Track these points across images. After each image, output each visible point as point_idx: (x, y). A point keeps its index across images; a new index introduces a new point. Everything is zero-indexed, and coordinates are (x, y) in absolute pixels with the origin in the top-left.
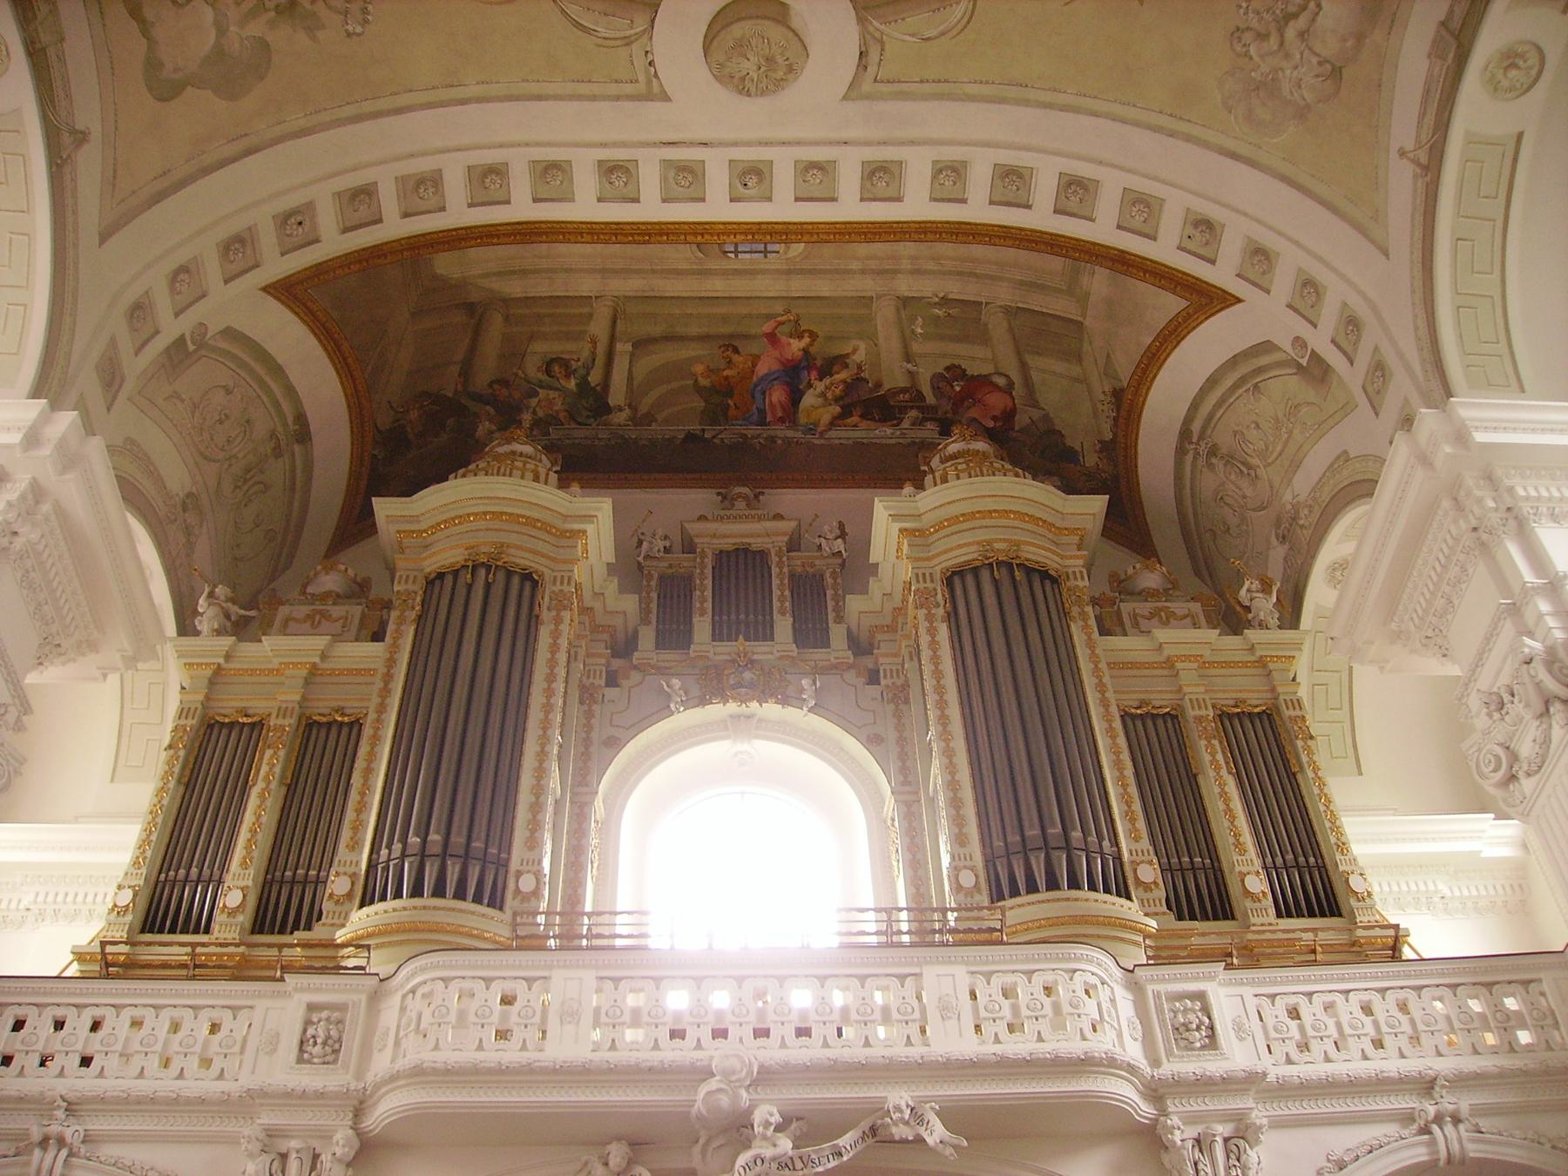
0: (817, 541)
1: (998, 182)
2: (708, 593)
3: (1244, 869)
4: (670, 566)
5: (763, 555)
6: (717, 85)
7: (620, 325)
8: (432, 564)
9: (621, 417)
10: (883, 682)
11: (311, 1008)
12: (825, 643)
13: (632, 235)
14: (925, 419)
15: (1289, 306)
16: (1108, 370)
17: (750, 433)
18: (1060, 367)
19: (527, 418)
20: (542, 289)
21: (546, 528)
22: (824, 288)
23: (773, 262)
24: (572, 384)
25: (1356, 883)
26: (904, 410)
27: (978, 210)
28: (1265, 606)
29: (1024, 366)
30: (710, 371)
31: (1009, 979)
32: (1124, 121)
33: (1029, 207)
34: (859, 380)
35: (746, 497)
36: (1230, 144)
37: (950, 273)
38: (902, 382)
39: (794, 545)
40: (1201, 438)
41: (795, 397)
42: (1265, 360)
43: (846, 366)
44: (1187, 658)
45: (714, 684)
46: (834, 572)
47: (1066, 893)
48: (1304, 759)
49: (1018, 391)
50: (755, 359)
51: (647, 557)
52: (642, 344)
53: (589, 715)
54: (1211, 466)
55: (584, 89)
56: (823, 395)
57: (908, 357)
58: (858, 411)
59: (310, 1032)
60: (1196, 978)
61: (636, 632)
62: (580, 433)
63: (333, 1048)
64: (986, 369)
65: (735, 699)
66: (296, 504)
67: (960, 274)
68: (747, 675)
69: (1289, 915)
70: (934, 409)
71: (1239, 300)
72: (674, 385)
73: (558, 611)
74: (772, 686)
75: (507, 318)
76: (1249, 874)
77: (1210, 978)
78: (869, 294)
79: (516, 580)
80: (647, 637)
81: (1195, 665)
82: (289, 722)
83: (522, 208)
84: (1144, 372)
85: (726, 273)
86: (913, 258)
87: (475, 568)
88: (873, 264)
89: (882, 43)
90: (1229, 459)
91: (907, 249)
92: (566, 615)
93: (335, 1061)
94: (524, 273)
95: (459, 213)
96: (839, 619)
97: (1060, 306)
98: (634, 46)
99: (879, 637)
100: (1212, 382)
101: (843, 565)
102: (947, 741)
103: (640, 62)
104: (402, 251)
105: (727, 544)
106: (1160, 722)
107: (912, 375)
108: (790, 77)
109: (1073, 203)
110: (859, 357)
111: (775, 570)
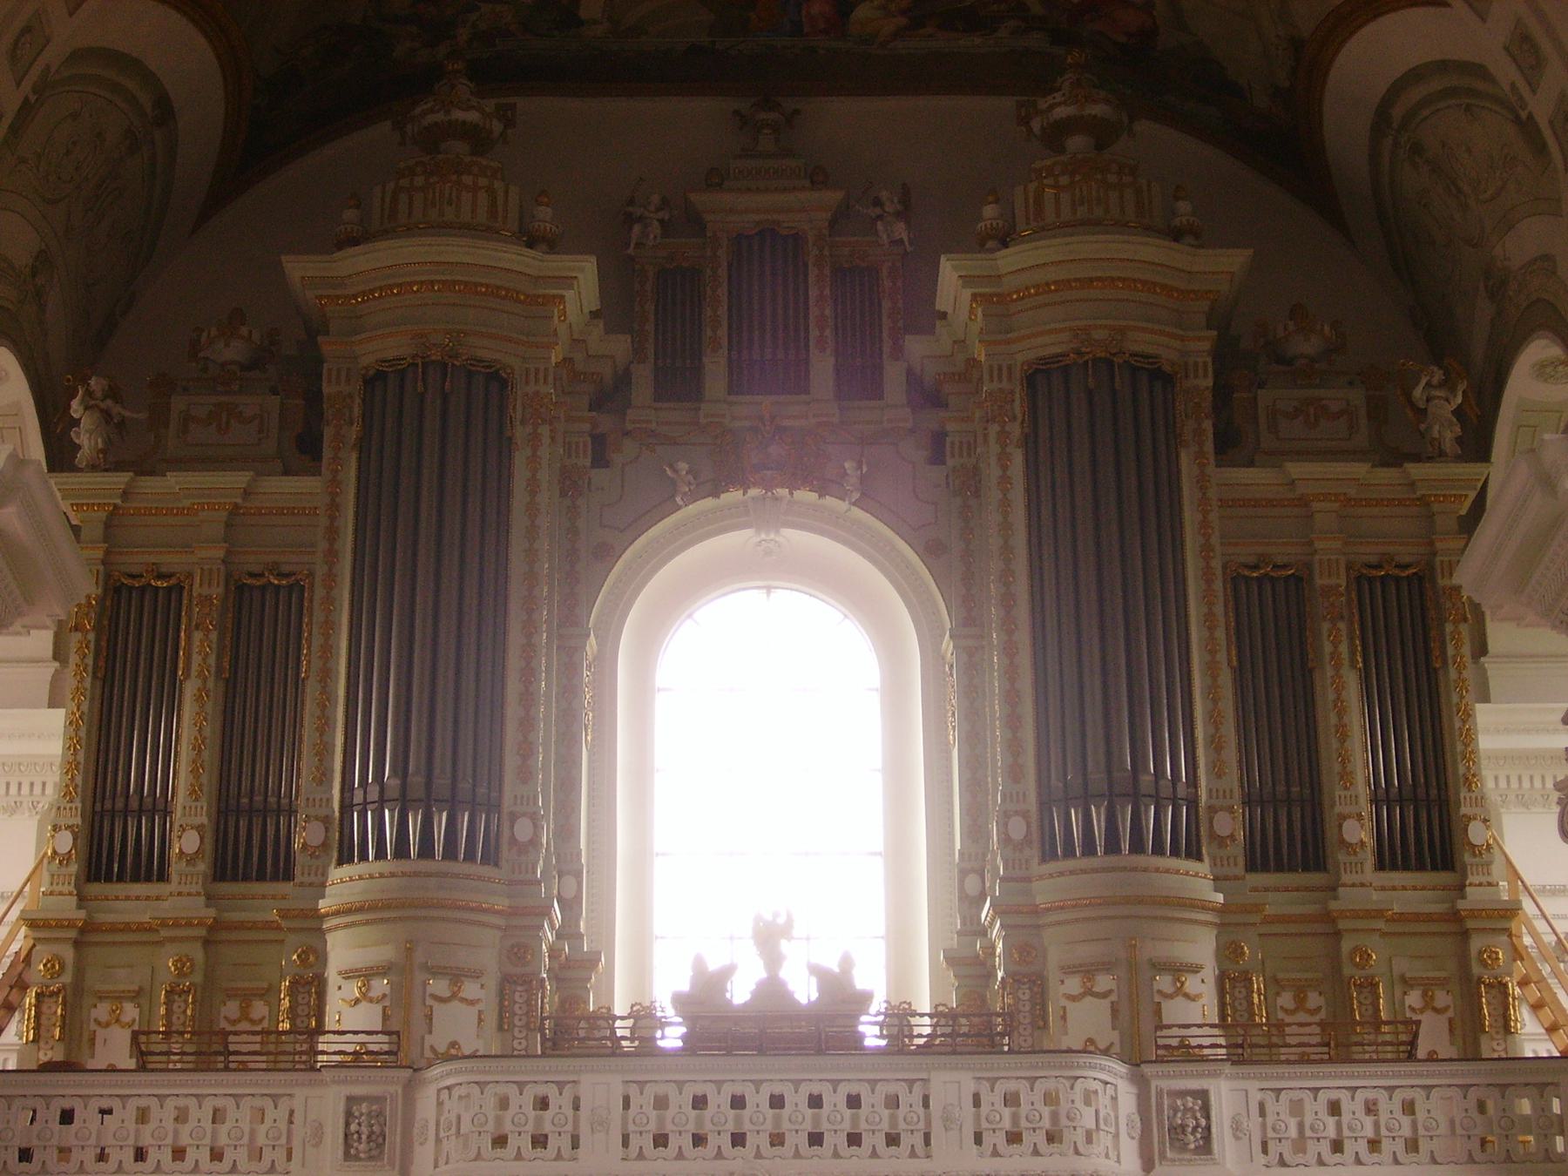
3: (1347, 810)
10: (950, 462)
11: (351, 1100)
15: (1506, 49)
25: (1476, 833)
28: (1443, 414)
31: (1012, 1086)
42: (1480, 85)
47: (1126, 858)
48: (1450, 651)
59: (353, 1127)
60: (1201, 1075)
61: (627, 373)
63: (377, 1141)
68: (774, 450)
69: (1394, 868)
77: (1215, 1075)
82: (217, 591)
93: (379, 1157)
100: (1415, 75)
102: (1010, 633)
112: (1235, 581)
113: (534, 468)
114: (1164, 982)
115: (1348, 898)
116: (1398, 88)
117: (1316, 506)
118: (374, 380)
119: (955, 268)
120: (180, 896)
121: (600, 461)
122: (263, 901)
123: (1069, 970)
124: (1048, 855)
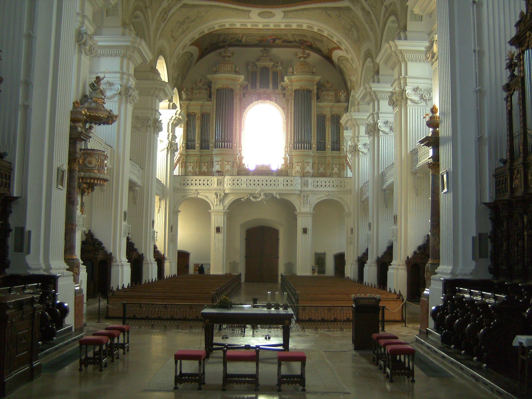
5: (268, 68)
45: (260, 97)
52: (247, 37)
53: (241, 103)
63: (221, 183)
74: (268, 98)
76: (329, 146)
80: (249, 86)
82: (200, 115)
112: (318, 116)
113: (236, 101)
114: (306, 164)
115: (328, 154)
118: (218, 90)
120: (196, 151)
121: (244, 96)
122: (206, 152)
123: (296, 162)
124: (294, 149)
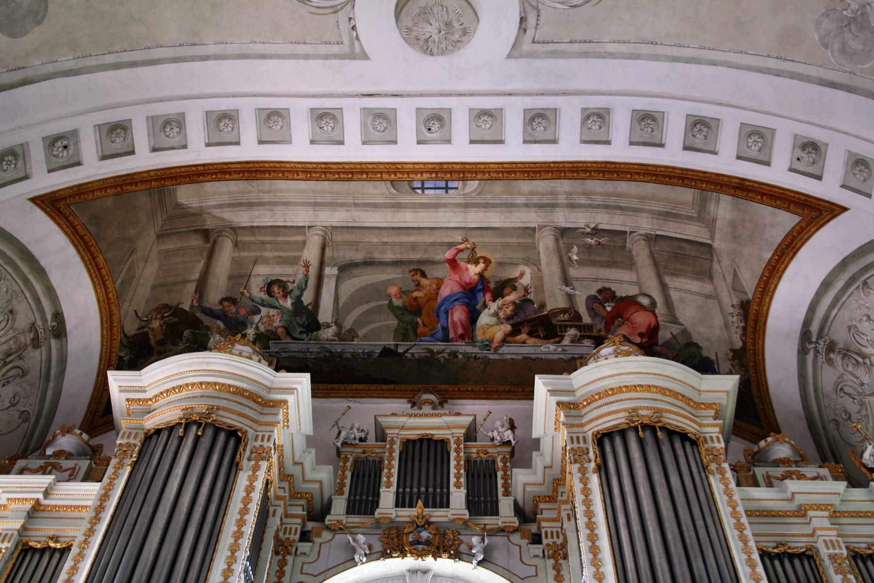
0: (490, 434)
1: (637, 126)
2: (395, 471)
4: (364, 452)
5: (443, 443)
6: (406, 46)
7: (328, 253)
8: (151, 423)
9: (328, 333)
10: (545, 541)
12: (495, 512)
13: (339, 173)
14: (583, 337)
16: (736, 287)
17: (435, 349)
18: (695, 286)
19: (251, 332)
20: (265, 219)
21: (253, 397)
22: (495, 219)
23: (453, 197)
24: (288, 303)
26: (564, 328)
27: (621, 151)
29: (664, 287)
30: (402, 293)
32: (738, 67)
33: (661, 145)
34: (525, 302)
35: (432, 403)
36: (829, 75)
37: (598, 206)
38: (562, 303)
39: (471, 434)
40: (820, 336)
41: (473, 316)
43: (515, 289)
44: (818, 507)
46: (504, 457)
49: (660, 310)
50: (440, 282)
51: (344, 444)
52: (346, 268)
53: (283, 563)
54: (830, 362)
55: (302, 49)
56: (496, 315)
57: (566, 280)
58: (526, 329)
61: (330, 501)
62: (294, 347)
64: (632, 291)
65: (412, 554)
66: (50, 393)
67: (607, 207)
68: (425, 535)
70: (589, 327)
71: (844, 209)
72: (373, 304)
73: (257, 461)
75: (236, 245)
78: (532, 225)
79: (222, 437)
80: (339, 505)
81: (826, 514)
83: (249, 150)
84: (767, 283)
85: (414, 207)
86: (569, 194)
87: (187, 426)
88: (535, 200)
89: (537, 9)
90: (846, 353)
91: (564, 186)
92: (264, 465)
94: (250, 205)
95: (198, 152)
96: (507, 493)
97: (693, 232)
98: (340, 13)
99: (542, 506)
101: (512, 454)
103: (345, 27)
104: (151, 181)
105: (413, 434)
106: (797, 562)
107: (570, 297)
108: (465, 38)
109: (699, 142)
110: (526, 280)
111: (453, 455)
116: (812, 308)
117: (811, 513)
119: (545, 384)
